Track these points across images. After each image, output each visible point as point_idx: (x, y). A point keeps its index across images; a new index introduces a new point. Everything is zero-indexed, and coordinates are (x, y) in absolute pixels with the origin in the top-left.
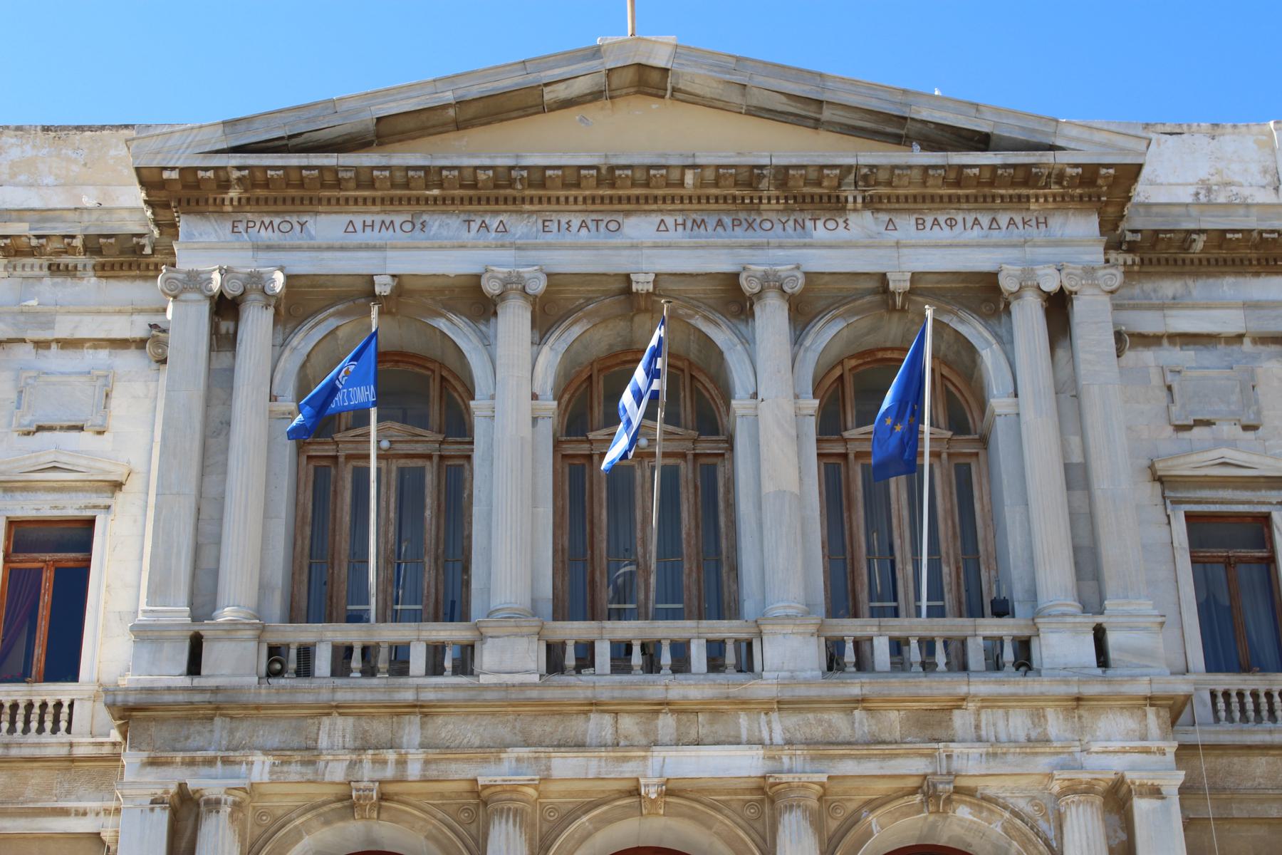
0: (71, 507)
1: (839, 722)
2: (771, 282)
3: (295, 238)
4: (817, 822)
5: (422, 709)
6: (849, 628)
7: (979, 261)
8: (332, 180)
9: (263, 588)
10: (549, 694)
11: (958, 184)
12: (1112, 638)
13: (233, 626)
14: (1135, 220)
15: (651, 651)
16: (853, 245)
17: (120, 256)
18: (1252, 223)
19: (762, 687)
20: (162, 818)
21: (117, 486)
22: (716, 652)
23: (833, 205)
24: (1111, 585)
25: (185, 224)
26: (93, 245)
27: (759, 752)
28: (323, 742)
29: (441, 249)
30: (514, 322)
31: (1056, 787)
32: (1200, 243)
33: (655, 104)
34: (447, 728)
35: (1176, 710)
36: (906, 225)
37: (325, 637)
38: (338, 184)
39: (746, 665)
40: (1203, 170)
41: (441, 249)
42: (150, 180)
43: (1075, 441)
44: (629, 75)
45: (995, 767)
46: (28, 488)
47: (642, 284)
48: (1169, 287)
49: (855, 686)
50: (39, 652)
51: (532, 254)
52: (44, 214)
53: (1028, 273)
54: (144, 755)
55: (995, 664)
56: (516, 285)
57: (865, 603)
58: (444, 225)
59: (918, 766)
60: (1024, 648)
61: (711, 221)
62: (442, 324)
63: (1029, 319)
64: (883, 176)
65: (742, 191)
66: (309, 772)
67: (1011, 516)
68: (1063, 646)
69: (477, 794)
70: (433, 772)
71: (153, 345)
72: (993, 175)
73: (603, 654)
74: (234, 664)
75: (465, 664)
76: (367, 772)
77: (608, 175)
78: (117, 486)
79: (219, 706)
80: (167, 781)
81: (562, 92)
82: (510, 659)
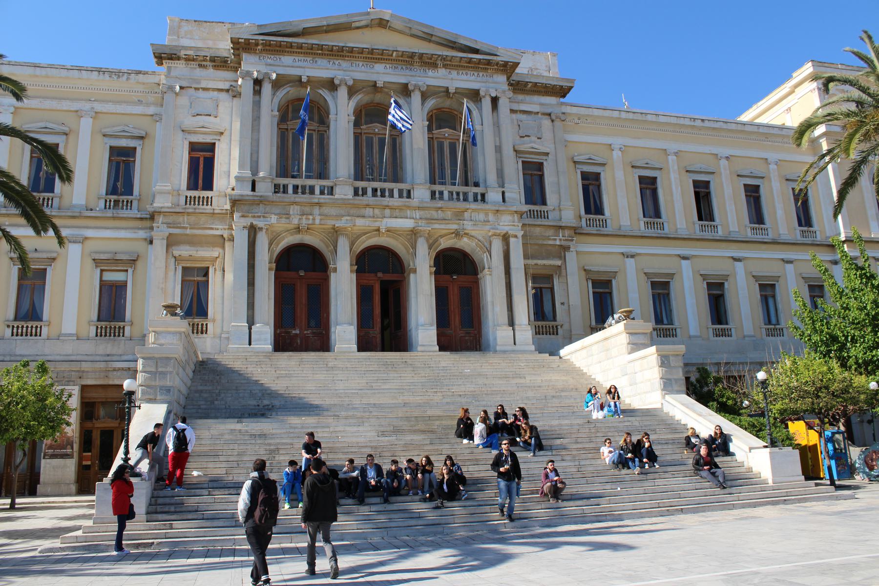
0: (208, 139)
1: (434, 214)
2: (417, 87)
3: (278, 62)
4: (427, 241)
5: (319, 204)
6: (438, 188)
7: (475, 86)
9: (271, 167)
10: (356, 202)
11: (469, 63)
12: (507, 195)
13: (264, 178)
14: (514, 77)
15: (383, 191)
16: (439, 78)
17: (220, 63)
18: (544, 81)
19: (415, 202)
20: (246, 232)
21: (222, 133)
22: (401, 192)
23: (434, 66)
24: (506, 181)
25: (245, 56)
26: (213, 59)
27: (413, 221)
28: (291, 213)
29: (322, 69)
30: (343, 92)
31: (490, 234)
32: (530, 85)
33: (383, 31)
34: (326, 210)
35: (521, 214)
36: (454, 73)
37: (291, 182)
38: (291, 47)
39: (409, 196)
41: (322, 69)
42: (235, 42)
43: (497, 139)
44: (377, 22)
45: (475, 228)
46: (195, 133)
47: (380, 84)
48: (520, 97)
49: (440, 204)
50: (200, 181)
51: (348, 73)
52: (198, 49)
53: (487, 91)
54: (240, 214)
55: (476, 200)
56: (343, 82)
57: (437, 181)
58: (322, 62)
59: (455, 227)
60: (483, 195)
61: (400, 67)
62: (321, 92)
63: (487, 103)
64: (449, 58)
65: (409, 59)
66: (287, 221)
67: (480, 159)
68: (494, 196)
69: (334, 229)
70: (323, 222)
71: (234, 92)
74: (265, 189)
76: (304, 221)
77: (372, 51)
78: (222, 133)
79: (262, 201)
80: (247, 222)
81: (357, 24)
82: (344, 192)
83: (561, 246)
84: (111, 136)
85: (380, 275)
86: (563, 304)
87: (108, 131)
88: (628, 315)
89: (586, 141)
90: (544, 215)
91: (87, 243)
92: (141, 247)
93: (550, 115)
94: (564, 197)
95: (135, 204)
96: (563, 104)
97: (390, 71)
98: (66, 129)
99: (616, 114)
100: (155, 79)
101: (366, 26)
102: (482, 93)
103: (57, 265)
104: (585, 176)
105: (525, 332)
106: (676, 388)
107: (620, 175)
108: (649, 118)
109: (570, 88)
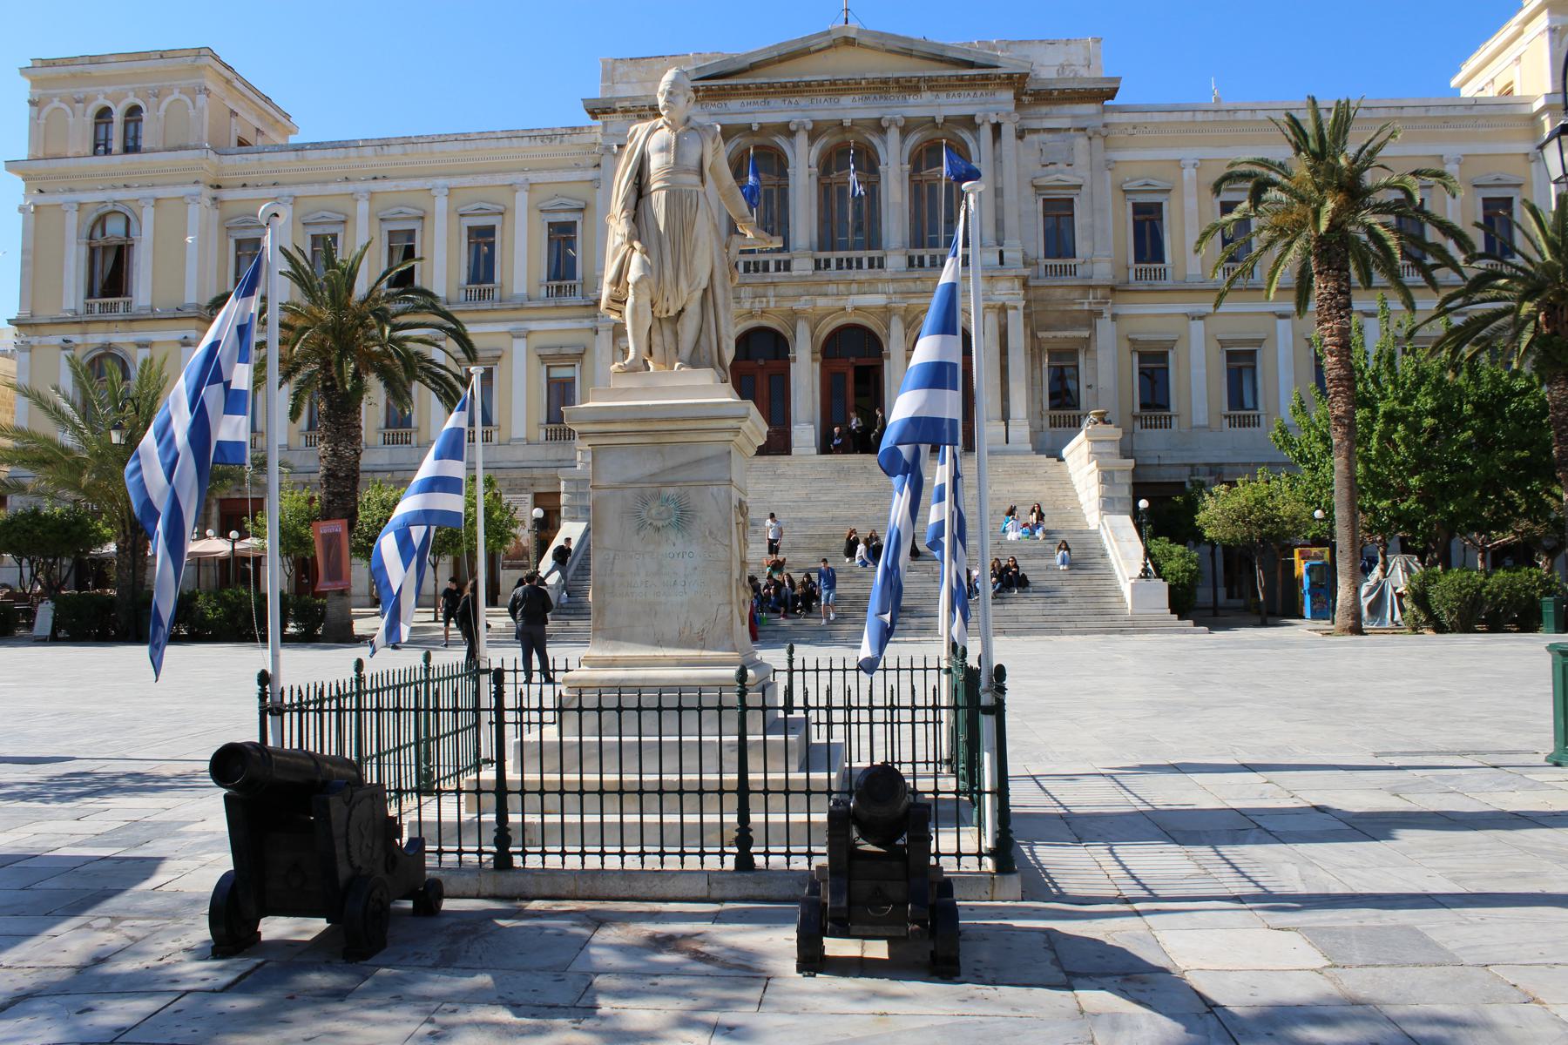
2: (893, 122)
4: (904, 319)
6: (917, 252)
7: (968, 111)
8: (734, 88)
12: (1006, 255)
15: (849, 261)
18: (1075, 86)
22: (871, 260)
23: (916, 89)
30: (802, 139)
33: (851, 49)
34: (782, 290)
36: (943, 95)
39: (881, 266)
40: (1061, 60)
47: (847, 123)
48: (1044, 109)
49: (917, 273)
52: (634, 99)
56: (801, 126)
58: (776, 102)
63: (986, 132)
65: (883, 87)
72: (973, 78)
73: (833, 263)
75: (788, 267)
76: (757, 305)
77: (833, 83)
82: (802, 266)
83: (1091, 311)
84: (548, 211)
85: (852, 360)
86: (1089, 387)
87: (545, 205)
88: (1103, 419)
89: (1140, 159)
90: (1070, 271)
91: (532, 337)
92: (585, 338)
93: (1084, 129)
94: (1103, 242)
95: (578, 288)
96: (1105, 110)
97: (859, 103)
98: (501, 208)
99: (1188, 116)
100: (586, 139)
101: (830, 47)
102: (978, 120)
103: (503, 362)
104: (1138, 209)
105: (1021, 430)
106: (1118, 507)
107: (1191, 203)
108: (1240, 115)
109: (1116, 90)
